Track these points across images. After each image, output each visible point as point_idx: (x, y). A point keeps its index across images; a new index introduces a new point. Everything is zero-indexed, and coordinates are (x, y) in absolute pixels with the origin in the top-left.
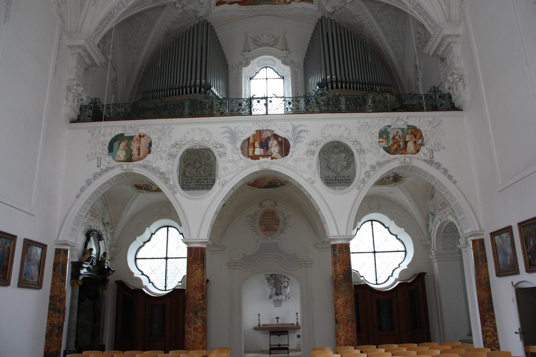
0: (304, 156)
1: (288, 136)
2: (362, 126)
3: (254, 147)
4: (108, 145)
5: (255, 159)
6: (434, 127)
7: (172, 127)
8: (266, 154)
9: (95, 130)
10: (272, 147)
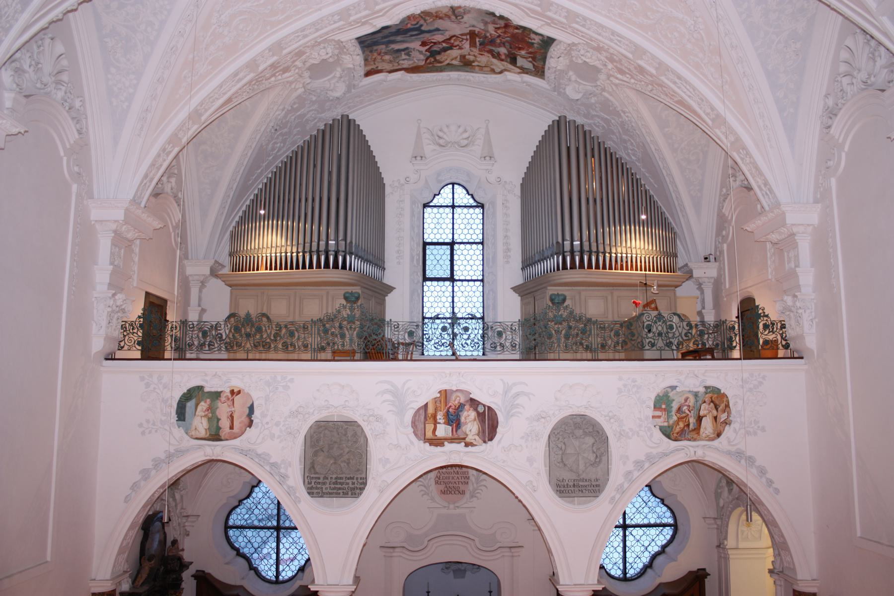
1: (495, 403)
2: (625, 386)
3: (436, 423)
4: (175, 406)
5: (436, 445)
8: (456, 436)
10: (466, 423)
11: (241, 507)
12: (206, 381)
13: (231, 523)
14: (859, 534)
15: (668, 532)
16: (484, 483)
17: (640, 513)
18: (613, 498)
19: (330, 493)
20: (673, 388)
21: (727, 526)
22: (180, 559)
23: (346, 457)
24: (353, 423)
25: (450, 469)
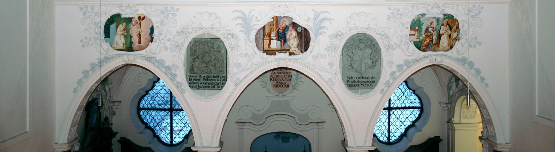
0: (326, 52)
1: (309, 26)
2: (392, 13)
3: (270, 39)
4: (103, 27)
5: (271, 54)
6: (473, 16)
7: (176, 8)
8: (283, 48)
9: (86, 7)
10: (290, 39)
11: (147, 96)
12: (123, 11)
13: (141, 106)
14: (537, 114)
15: (417, 112)
16: (301, 80)
17: (400, 100)
18: (383, 90)
19: (204, 87)
20: (423, 15)
21: (454, 109)
22: (111, 130)
23: (214, 62)
24: (217, 39)
25: (279, 71)
